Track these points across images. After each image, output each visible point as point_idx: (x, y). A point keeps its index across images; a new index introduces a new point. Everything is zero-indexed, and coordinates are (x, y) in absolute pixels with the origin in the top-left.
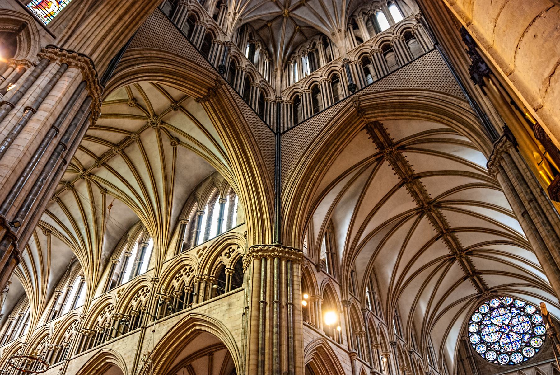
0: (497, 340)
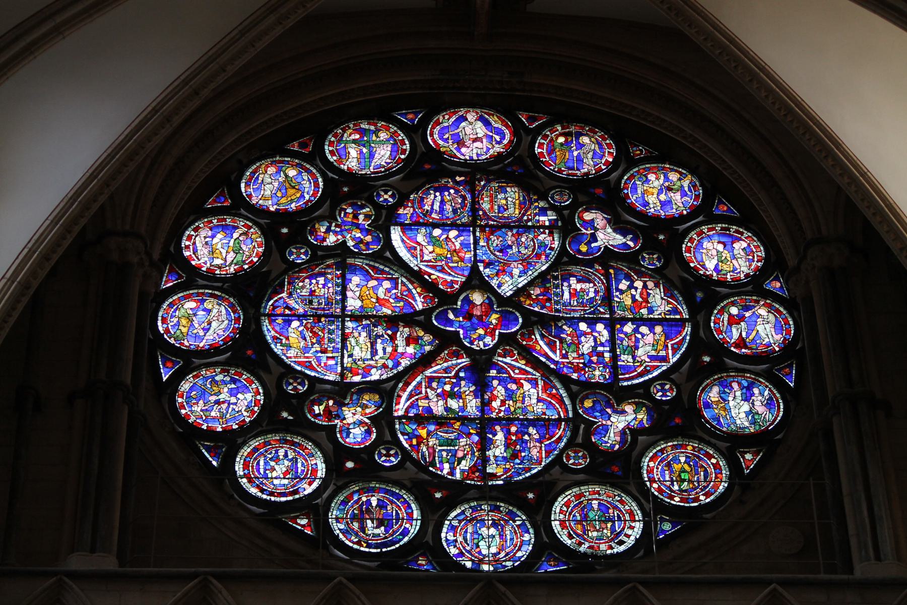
0: (375, 375)
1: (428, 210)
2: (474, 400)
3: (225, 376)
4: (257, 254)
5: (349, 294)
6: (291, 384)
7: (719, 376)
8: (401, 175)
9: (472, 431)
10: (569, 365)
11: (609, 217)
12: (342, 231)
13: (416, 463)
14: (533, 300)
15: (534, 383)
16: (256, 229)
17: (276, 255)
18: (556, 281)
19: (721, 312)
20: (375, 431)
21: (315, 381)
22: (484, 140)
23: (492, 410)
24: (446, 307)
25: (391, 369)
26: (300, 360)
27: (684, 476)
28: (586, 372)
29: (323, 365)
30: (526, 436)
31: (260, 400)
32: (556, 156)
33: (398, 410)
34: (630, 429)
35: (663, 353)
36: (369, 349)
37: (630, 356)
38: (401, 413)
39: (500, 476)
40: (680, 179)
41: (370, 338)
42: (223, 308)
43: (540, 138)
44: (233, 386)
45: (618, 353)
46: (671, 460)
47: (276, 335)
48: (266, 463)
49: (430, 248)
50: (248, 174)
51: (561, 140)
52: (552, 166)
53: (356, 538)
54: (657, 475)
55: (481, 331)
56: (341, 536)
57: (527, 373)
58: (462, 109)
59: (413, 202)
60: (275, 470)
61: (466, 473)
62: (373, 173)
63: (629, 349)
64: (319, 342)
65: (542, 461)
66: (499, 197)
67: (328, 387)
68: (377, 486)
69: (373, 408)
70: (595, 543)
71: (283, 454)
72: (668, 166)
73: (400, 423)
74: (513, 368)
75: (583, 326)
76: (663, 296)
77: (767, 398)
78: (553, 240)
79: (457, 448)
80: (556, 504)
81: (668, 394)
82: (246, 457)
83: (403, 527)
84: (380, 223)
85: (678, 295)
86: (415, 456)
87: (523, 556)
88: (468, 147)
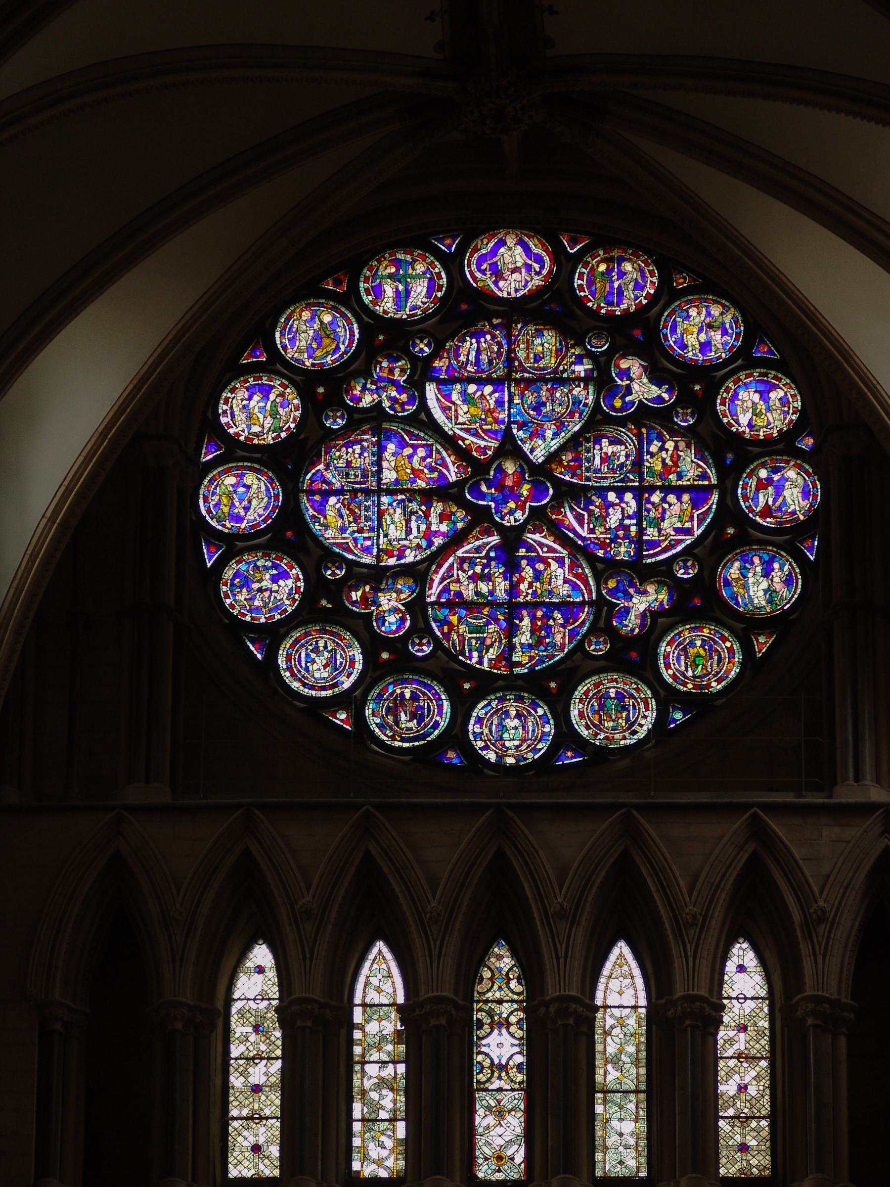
1: (463, 362)
2: (503, 582)
3: (266, 561)
4: (294, 419)
5: (385, 464)
6: (329, 569)
7: (742, 549)
9: (500, 617)
10: (596, 541)
11: (646, 364)
12: (377, 389)
13: (447, 651)
14: (565, 467)
15: (560, 562)
16: (293, 389)
19: (750, 476)
21: (351, 564)
22: (523, 270)
23: (518, 593)
24: (478, 478)
25: (425, 549)
26: (338, 541)
27: (699, 661)
28: (611, 549)
29: (359, 546)
30: (551, 620)
31: (300, 587)
32: (596, 289)
33: (431, 595)
35: (688, 525)
36: (404, 528)
38: (433, 598)
39: (524, 665)
40: (722, 314)
41: (405, 515)
42: (263, 483)
43: (580, 266)
44: (275, 572)
45: (644, 526)
46: (687, 644)
47: (315, 513)
48: (307, 655)
49: (465, 408)
50: (283, 320)
51: (603, 267)
54: (673, 660)
55: (512, 505)
57: (555, 551)
58: (501, 230)
59: (448, 352)
62: (409, 316)
63: (656, 521)
64: (355, 521)
66: (535, 342)
67: (365, 570)
68: (411, 677)
69: (408, 593)
70: (611, 733)
71: (323, 645)
72: (711, 297)
73: (432, 609)
74: (541, 545)
75: (612, 497)
76: (693, 458)
77: (787, 573)
79: (485, 635)
80: (576, 693)
83: (434, 720)
84: (415, 378)
85: (709, 457)
86: (446, 644)
87: (543, 748)
88: (506, 280)
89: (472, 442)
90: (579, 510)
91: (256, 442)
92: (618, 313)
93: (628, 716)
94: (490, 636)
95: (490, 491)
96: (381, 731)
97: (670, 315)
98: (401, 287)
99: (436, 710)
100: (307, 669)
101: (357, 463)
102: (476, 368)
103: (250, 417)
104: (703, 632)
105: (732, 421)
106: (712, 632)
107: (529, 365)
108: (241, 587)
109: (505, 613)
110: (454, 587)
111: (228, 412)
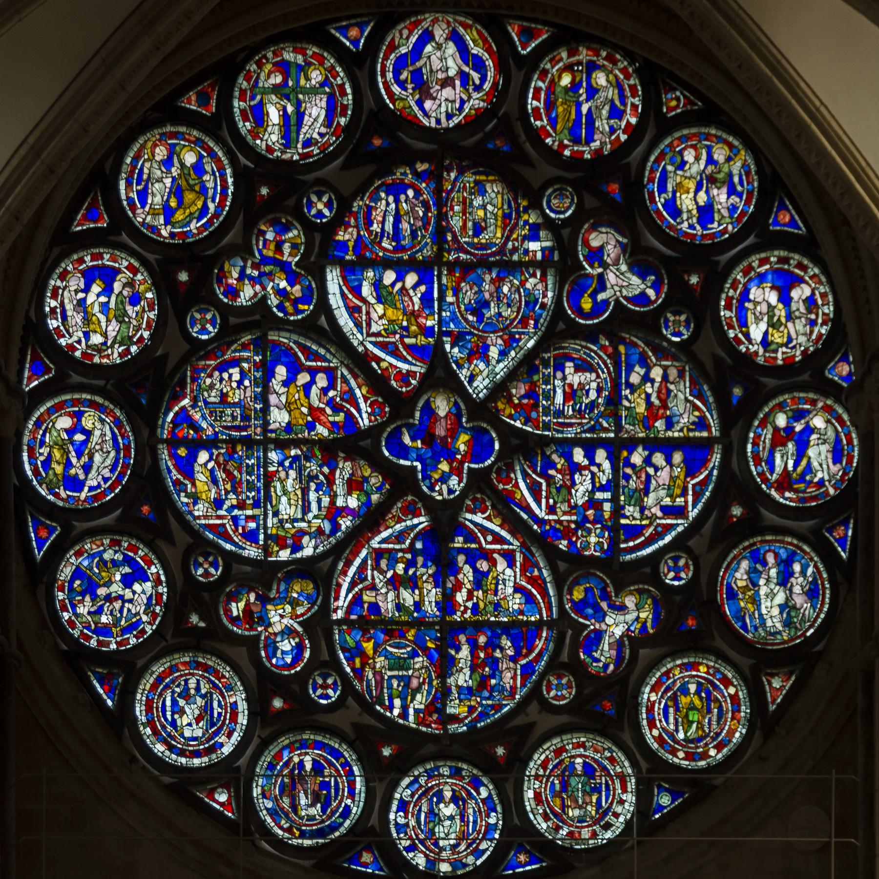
1: (377, 233)
2: (434, 590)
3: (116, 552)
4: (148, 322)
5: (273, 399)
6: (201, 565)
7: (751, 541)
8: (342, 159)
9: (430, 645)
10: (558, 526)
11: (625, 241)
12: (261, 274)
13: (359, 697)
14: (515, 407)
16: (145, 274)
17: (173, 323)
18: (546, 369)
19: (763, 424)
20: (308, 646)
21: (232, 559)
25: (329, 536)
26: (211, 522)
27: (694, 716)
28: (578, 538)
30: (498, 651)
31: (162, 594)
33: (338, 608)
34: (629, 637)
35: (680, 501)
36: (300, 503)
37: (638, 508)
38: (340, 614)
40: (729, 159)
41: (301, 482)
42: (108, 427)
43: (536, 76)
44: (127, 570)
45: (622, 503)
46: (678, 689)
47: (179, 477)
48: (174, 702)
49: (380, 309)
50: (128, 160)
51: (566, 80)
52: (550, 135)
53: (287, 822)
54: (659, 714)
55: (444, 466)
56: (269, 820)
58: (427, 15)
60: (185, 712)
61: (422, 715)
62: (303, 156)
63: (637, 495)
64: (234, 490)
65: (515, 693)
66: (474, 203)
68: (312, 737)
70: (577, 827)
72: (713, 132)
73: (340, 631)
74: (485, 531)
75: (579, 455)
76: (688, 395)
77: (810, 579)
78: (547, 290)
79: (410, 672)
80: (532, 764)
81: (683, 575)
82: (149, 692)
83: (343, 805)
85: (709, 393)
87: (487, 849)
89: (391, 365)
90: (534, 476)
91: (96, 360)
92: (587, 156)
93: (599, 800)
94: (416, 674)
95: (414, 444)
96: (274, 820)
97: (658, 161)
98: (290, 109)
99: (346, 789)
100: (173, 723)
101: (235, 397)
102: (394, 244)
103: (87, 319)
104: (698, 671)
105: (740, 335)
106: (711, 671)
107: (467, 239)
108: (83, 594)
109: (437, 639)
110: (368, 597)
111: (58, 310)
